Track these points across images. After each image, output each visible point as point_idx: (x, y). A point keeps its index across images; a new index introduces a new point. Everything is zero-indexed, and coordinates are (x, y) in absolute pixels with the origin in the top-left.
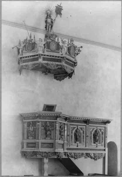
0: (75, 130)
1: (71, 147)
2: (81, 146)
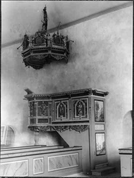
0: (59, 105)
1: (56, 121)
2: (64, 119)
